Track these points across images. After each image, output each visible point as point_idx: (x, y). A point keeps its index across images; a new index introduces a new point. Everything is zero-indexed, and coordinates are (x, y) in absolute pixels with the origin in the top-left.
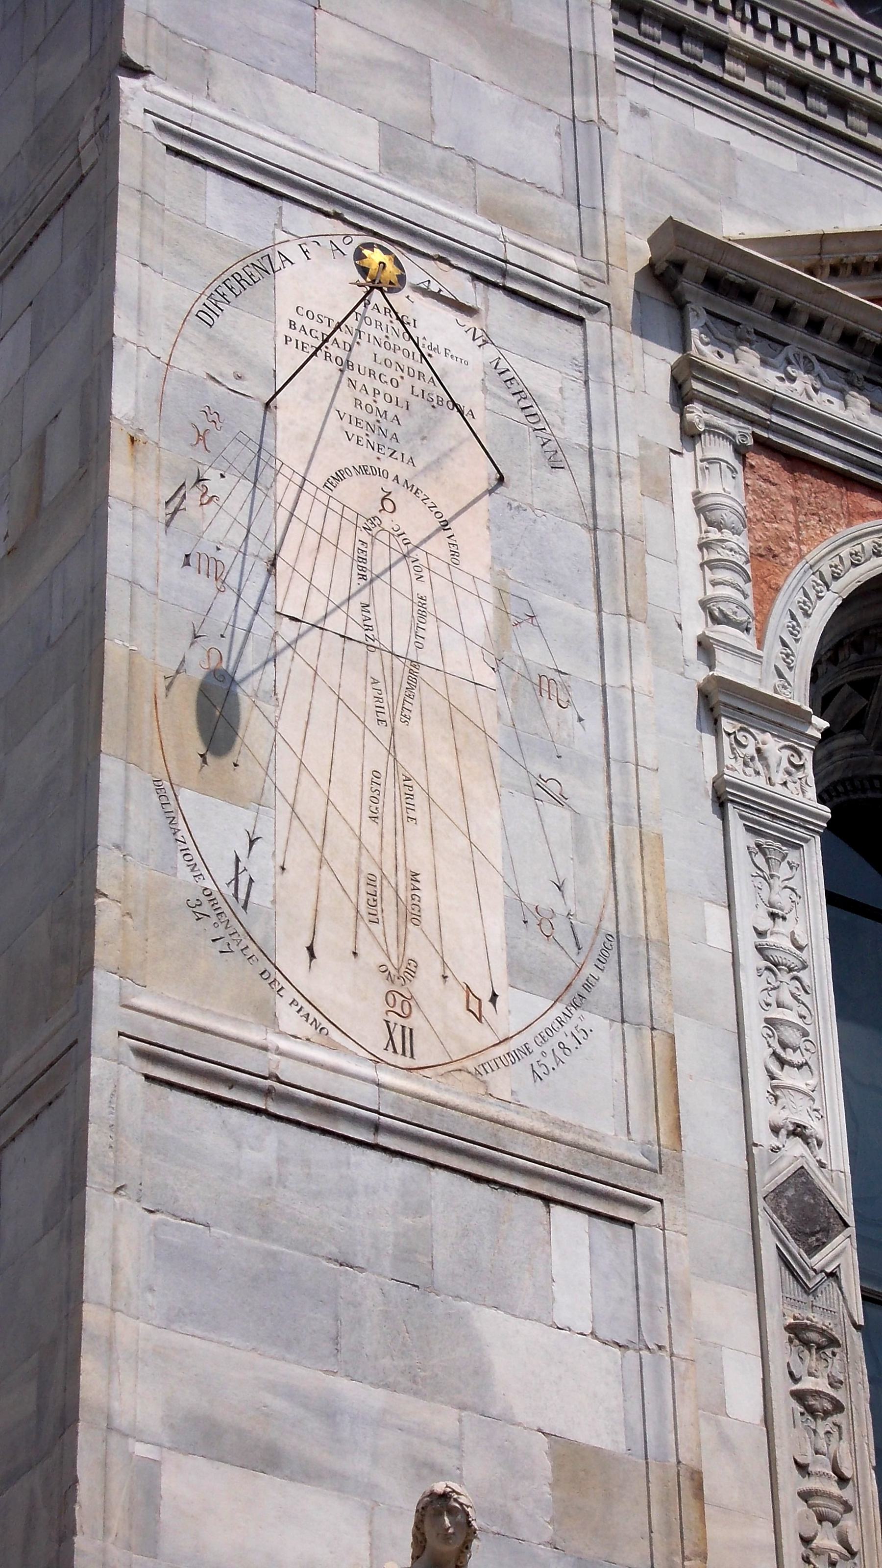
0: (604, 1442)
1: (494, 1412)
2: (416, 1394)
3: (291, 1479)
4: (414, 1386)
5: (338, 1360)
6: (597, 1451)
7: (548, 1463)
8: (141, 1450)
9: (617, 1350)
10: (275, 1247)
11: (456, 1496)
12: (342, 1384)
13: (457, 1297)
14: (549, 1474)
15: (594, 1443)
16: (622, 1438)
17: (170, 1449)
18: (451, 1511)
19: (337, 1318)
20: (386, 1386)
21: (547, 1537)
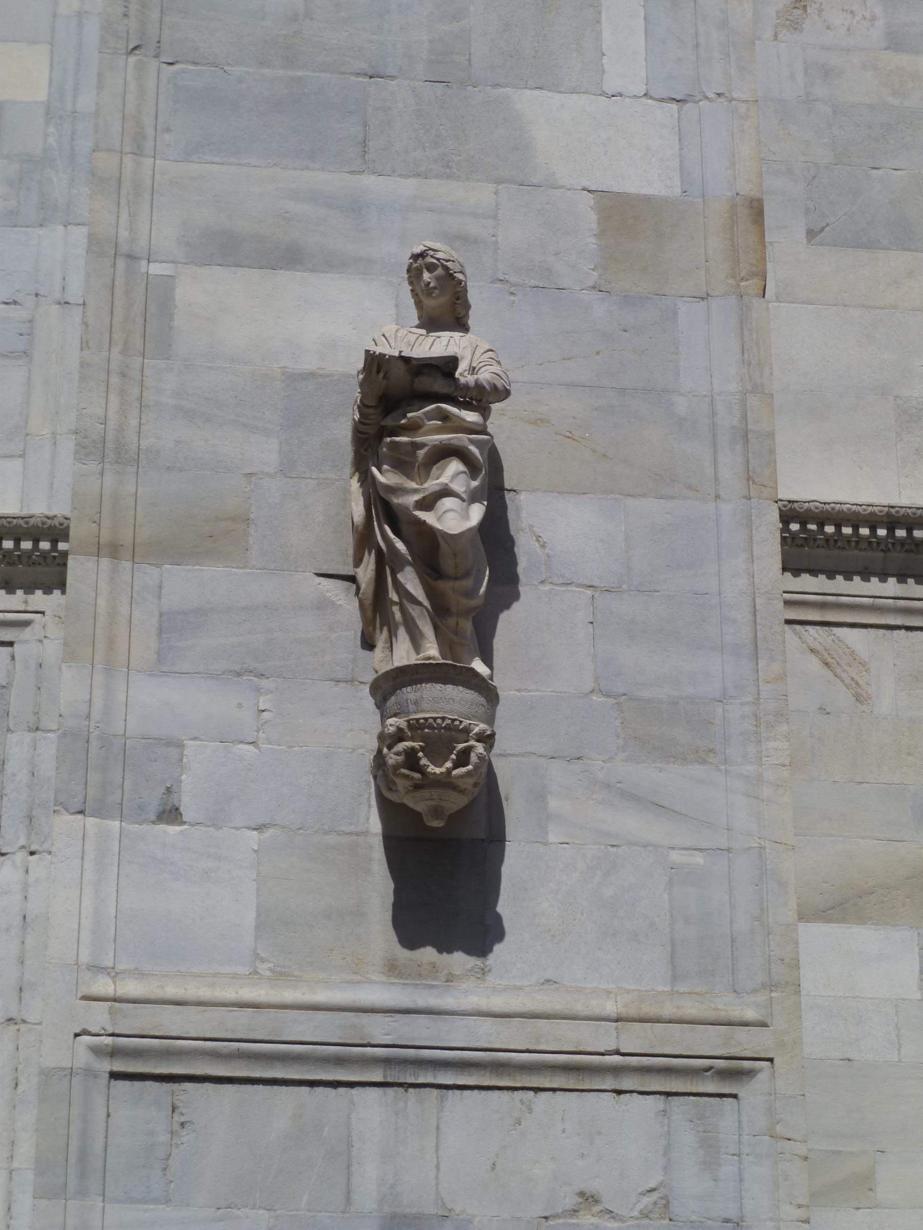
0: (656, 189)
1: (535, 181)
2: (449, 177)
3: (312, 271)
4: (448, 170)
5: (365, 160)
6: (647, 199)
7: (593, 217)
8: (155, 269)
9: (674, 106)
10: (300, 73)
11: (432, 253)
12: (369, 181)
13: (498, 85)
14: (594, 226)
15: (645, 191)
16: (677, 182)
17: (185, 263)
18: (431, 268)
19: (365, 125)
20: (418, 175)
21: (590, 283)
